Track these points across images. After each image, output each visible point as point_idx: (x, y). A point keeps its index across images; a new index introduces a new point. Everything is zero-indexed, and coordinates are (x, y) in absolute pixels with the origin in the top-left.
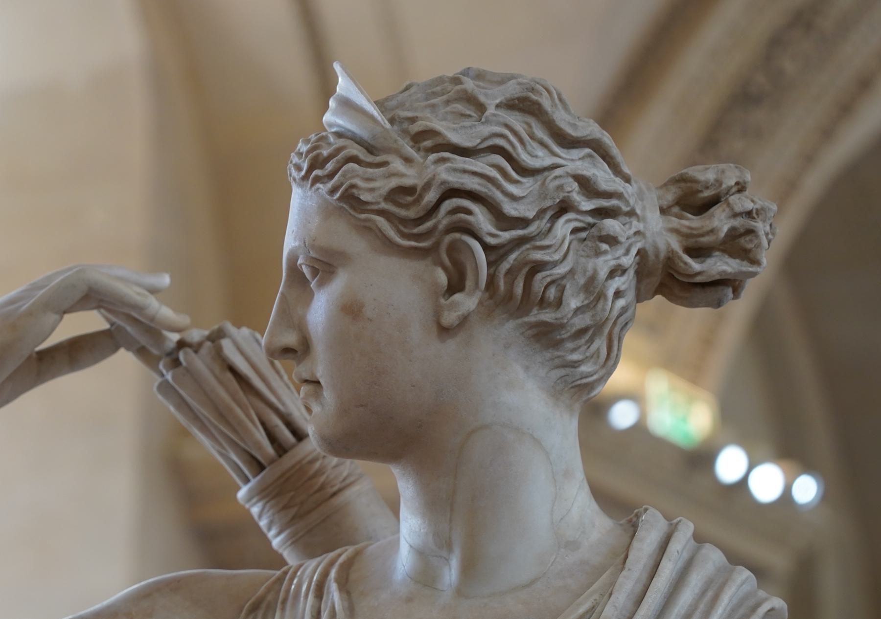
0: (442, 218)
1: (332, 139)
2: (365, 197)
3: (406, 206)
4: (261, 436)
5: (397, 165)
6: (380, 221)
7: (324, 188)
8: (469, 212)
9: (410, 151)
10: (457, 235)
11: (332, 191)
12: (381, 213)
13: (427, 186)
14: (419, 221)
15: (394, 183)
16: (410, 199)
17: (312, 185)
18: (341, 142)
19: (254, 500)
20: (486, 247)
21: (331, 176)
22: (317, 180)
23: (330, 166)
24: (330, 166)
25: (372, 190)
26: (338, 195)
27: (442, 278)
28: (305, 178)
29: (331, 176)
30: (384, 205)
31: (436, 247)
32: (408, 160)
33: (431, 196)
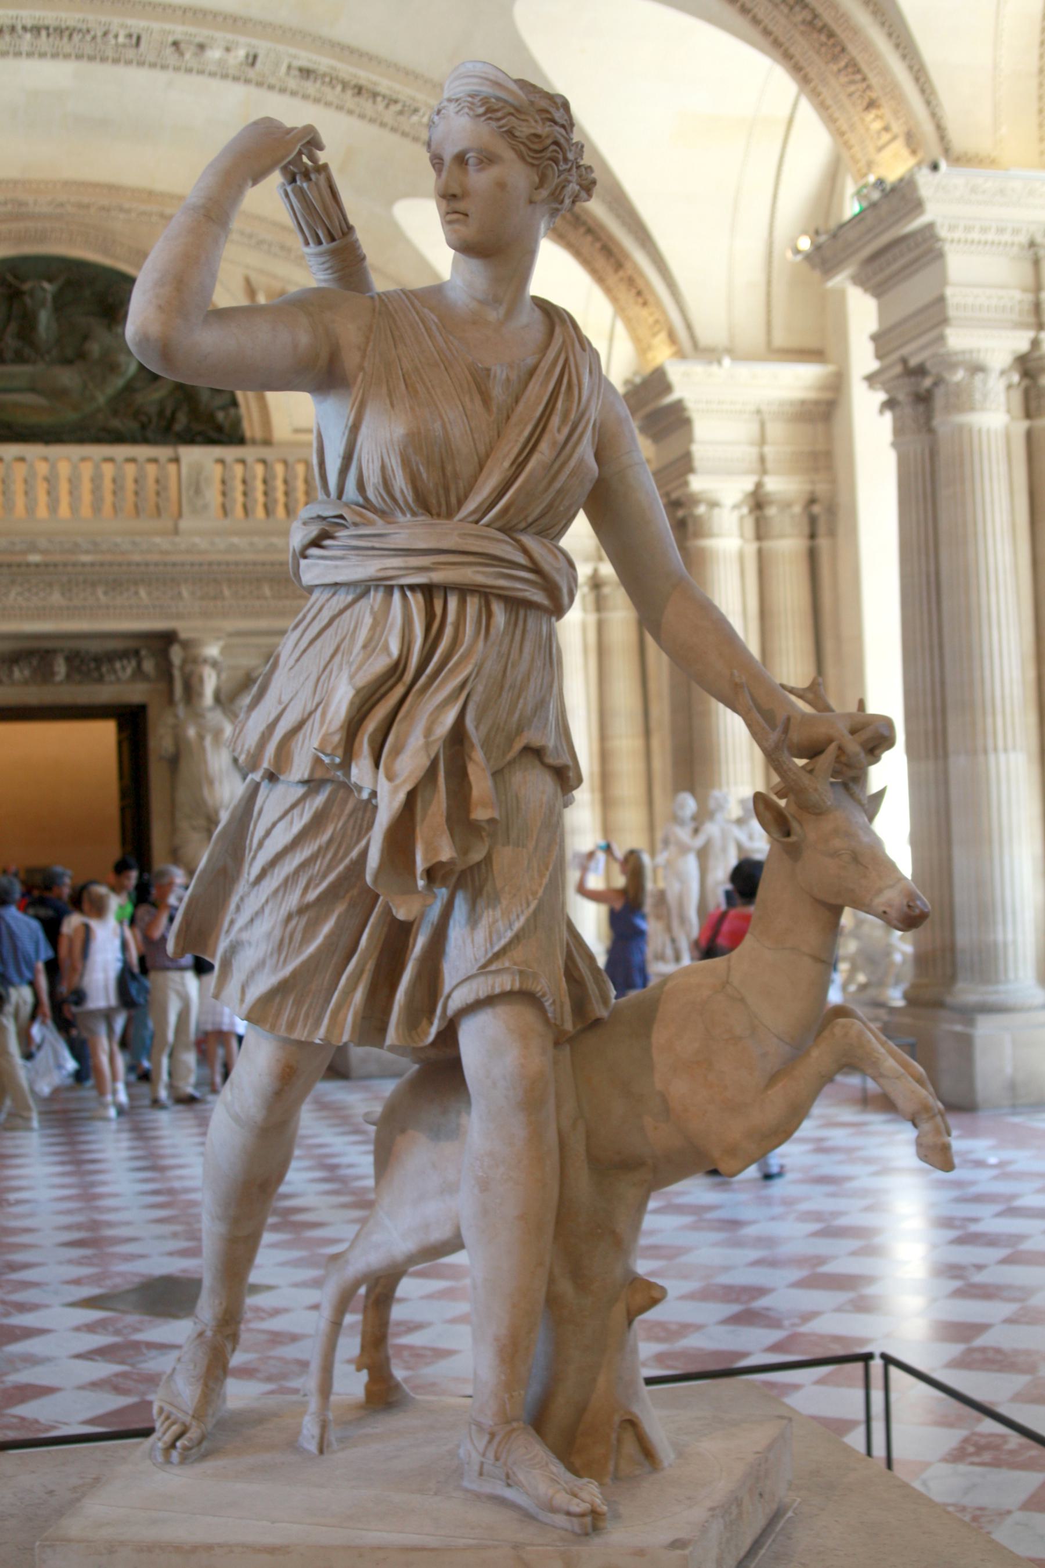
0: (548, 154)
1: (493, 100)
2: (517, 134)
3: (533, 143)
4: (337, 223)
5: (533, 124)
6: (522, 148)
7: (494, 124)
8: (558, 153)
9: (538, 118)
10: (551, 162)
11: (501, 127)
12: (523, 143)
13: (548, 137)
14: (541, 151)
15: (533, 131)
16: (536, 140)
17: (486, 120)
18: (501, 104)
19: (326, 255)
20: (558, 170)
21: (498, 119)
22: (490, 118)
23: (499, 114)
24: (499, 114)
25: (521, 131)
26: (504, 129)
27: (537, 179)
28: (479, 116)
29: (498, 119)
30: (525, 141)
31: (538, 166)
32: (536, 121)
33: (549, 141)
